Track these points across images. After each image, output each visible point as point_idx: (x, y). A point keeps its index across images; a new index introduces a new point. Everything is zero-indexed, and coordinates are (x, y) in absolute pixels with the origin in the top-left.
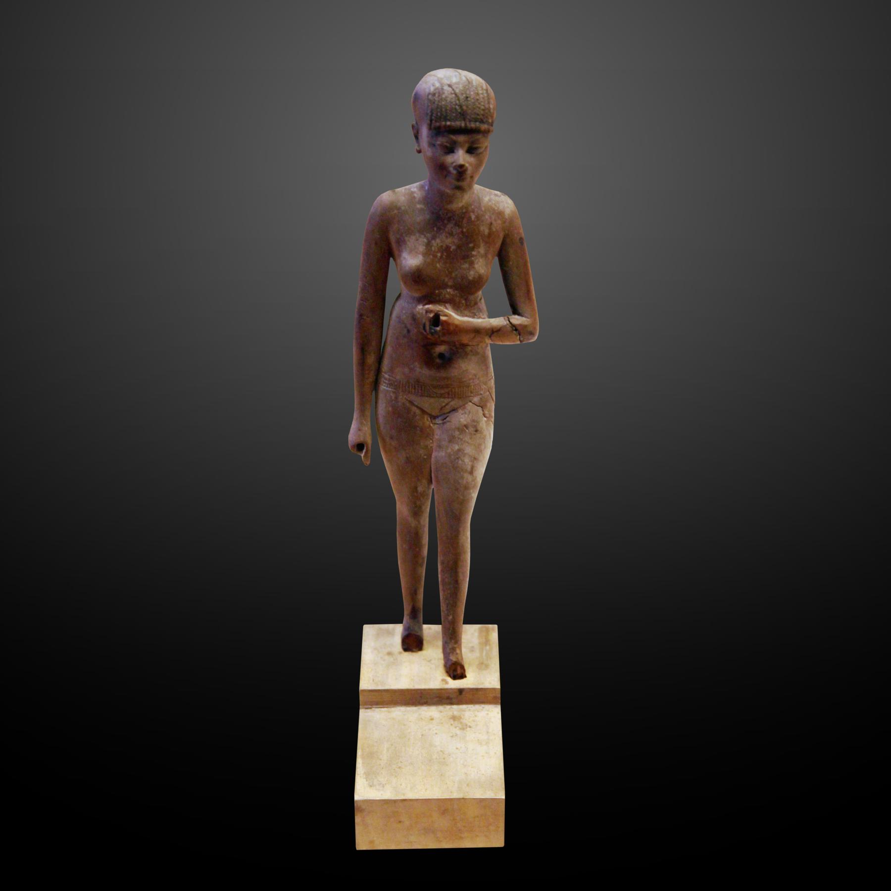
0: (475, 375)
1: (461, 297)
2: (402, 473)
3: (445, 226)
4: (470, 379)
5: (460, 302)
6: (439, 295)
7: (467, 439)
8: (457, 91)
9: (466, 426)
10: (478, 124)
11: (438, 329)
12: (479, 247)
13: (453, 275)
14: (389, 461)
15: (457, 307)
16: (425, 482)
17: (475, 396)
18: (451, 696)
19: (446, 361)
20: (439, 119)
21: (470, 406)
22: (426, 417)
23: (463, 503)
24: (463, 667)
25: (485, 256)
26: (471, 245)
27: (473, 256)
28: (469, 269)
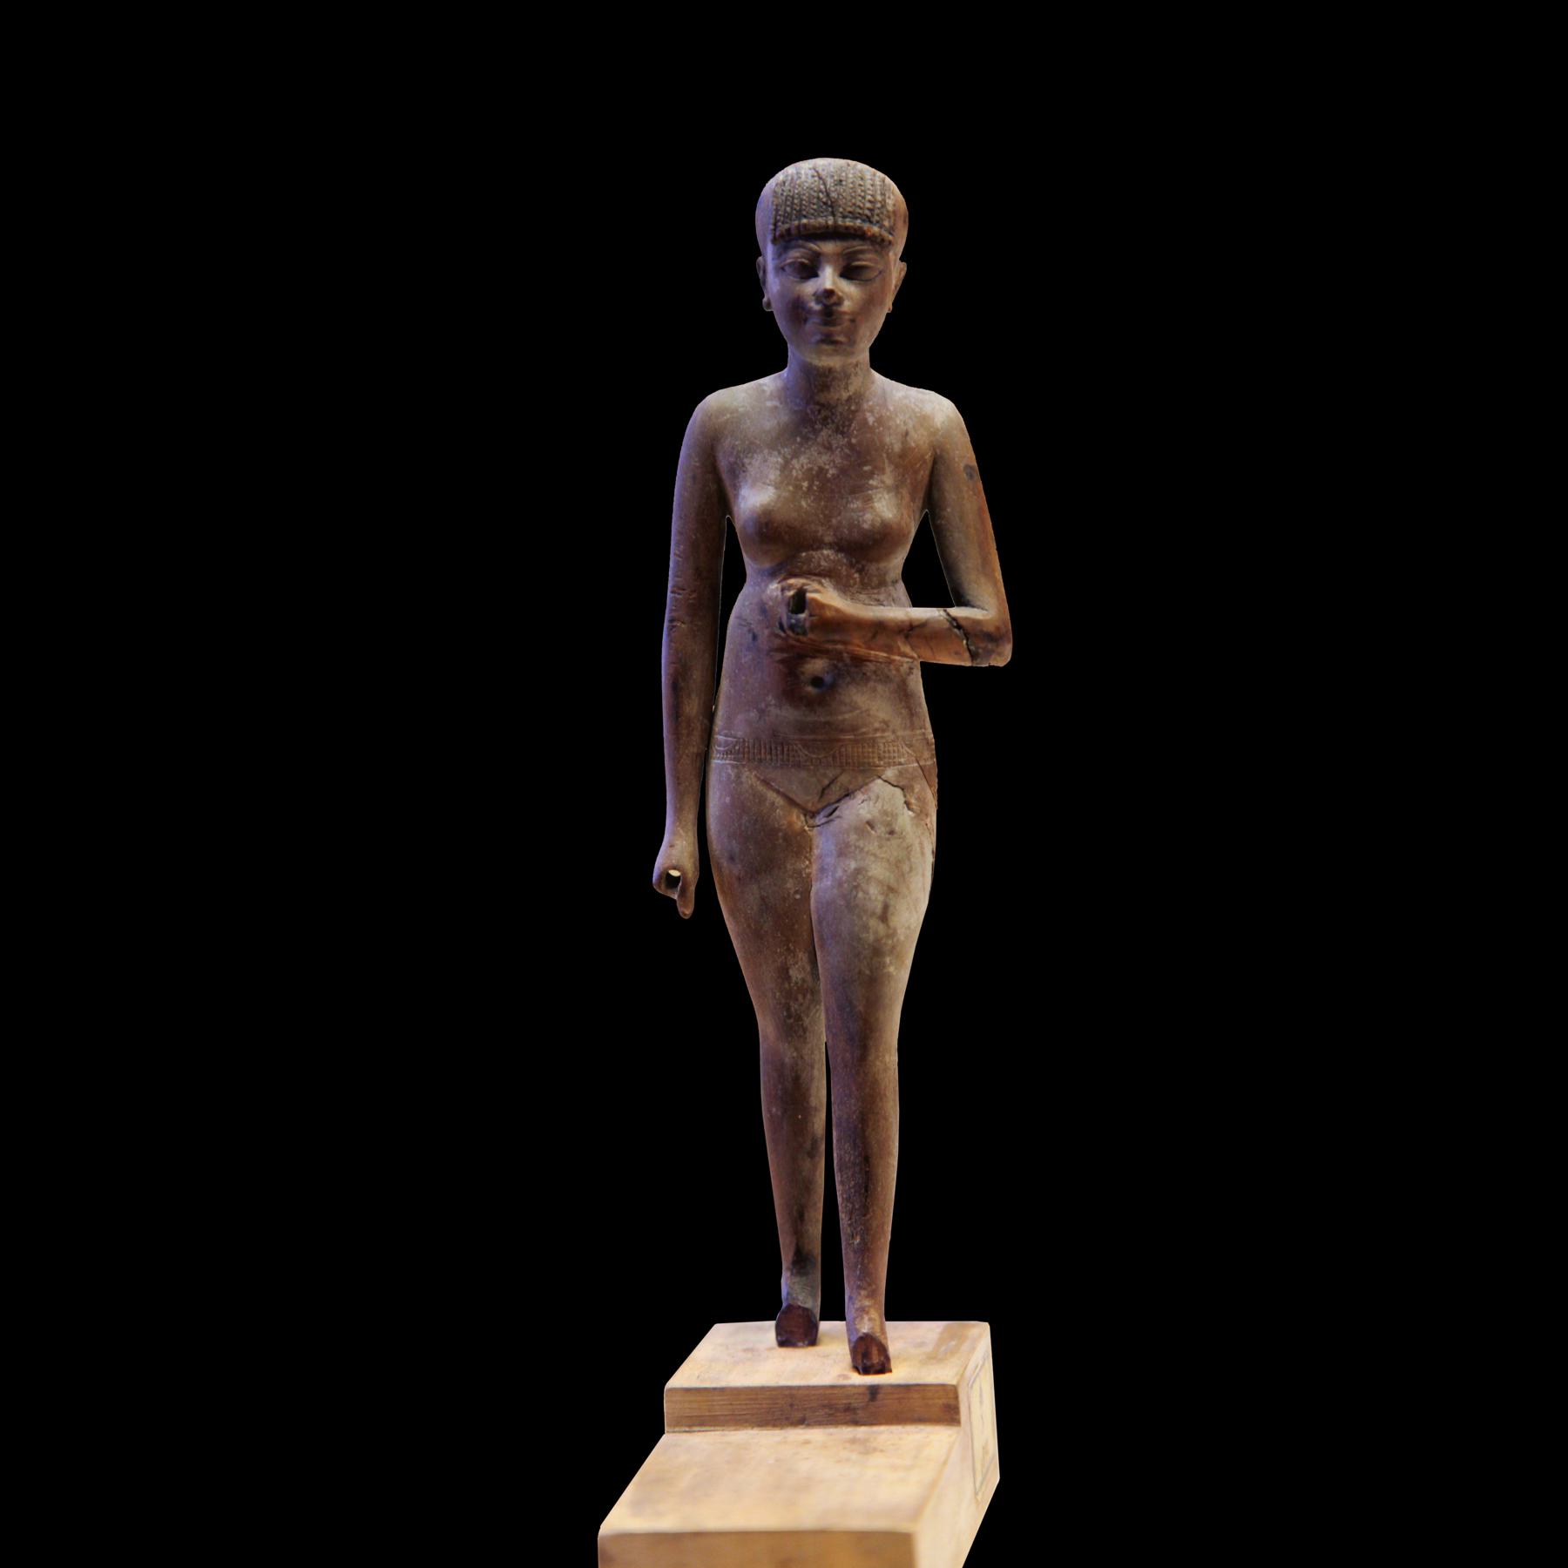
0: (886, 723)
1: (852, 565)
2: (756, 935)
3: (816, 432)
4: (876, 730)
5: (849, 576)
6: (809, 560)
7: (873, 847)
8: (823, 174)
9: (870, 824)
10: (858, 222)
11: (802, 616)
12: (883, 471)
13: (834, 521)
14: (732, 912)
15: (844, 587)
16: (802, 956)
17: (889, 765)
18: (855, 1403)
19: (826, 689)
20: (787, 216)
21: (878, 786)
22: (795, 812)
23: (874, 981)
24: (883, 1350)
25: (896, 489)
26: (866, 468)
27: (872, 488)
28: (863, 510)
